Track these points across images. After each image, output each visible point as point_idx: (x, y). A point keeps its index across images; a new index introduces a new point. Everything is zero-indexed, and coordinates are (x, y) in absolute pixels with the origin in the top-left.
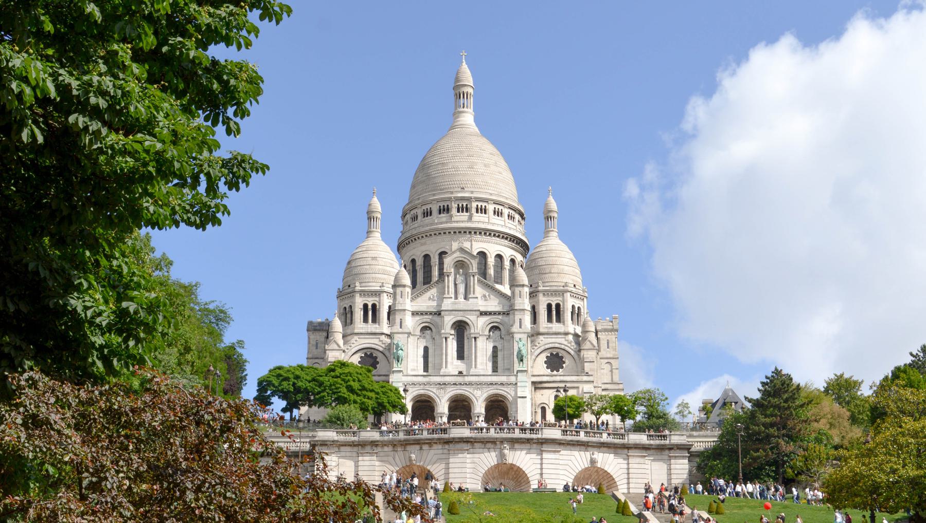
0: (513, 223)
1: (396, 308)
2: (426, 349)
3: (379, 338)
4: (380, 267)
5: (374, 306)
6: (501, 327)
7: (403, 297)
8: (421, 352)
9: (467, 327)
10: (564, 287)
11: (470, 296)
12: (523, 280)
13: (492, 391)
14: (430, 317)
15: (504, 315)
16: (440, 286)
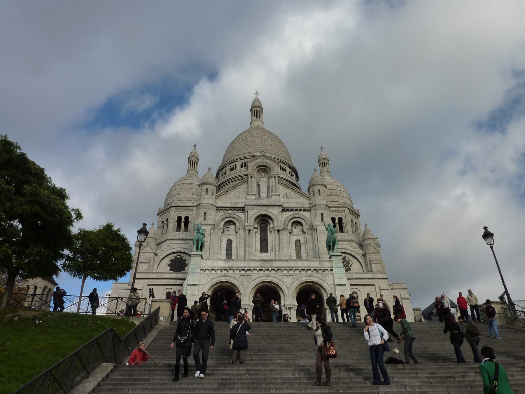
0: (292, 177)
1: (201, 203)
2: (229, 242)
3: (189, 244)
4: (194, 190)
5: (187, 218)
6: (302, 221)
7: (208, 193)
8: (224, 244)
9: (270, 222)
10: (344, 205)
11: (273, 194)
12: (320, 181)
13: (305, 277)
14: (235, 212)
15: (305, 212)
16: (243, 186)
